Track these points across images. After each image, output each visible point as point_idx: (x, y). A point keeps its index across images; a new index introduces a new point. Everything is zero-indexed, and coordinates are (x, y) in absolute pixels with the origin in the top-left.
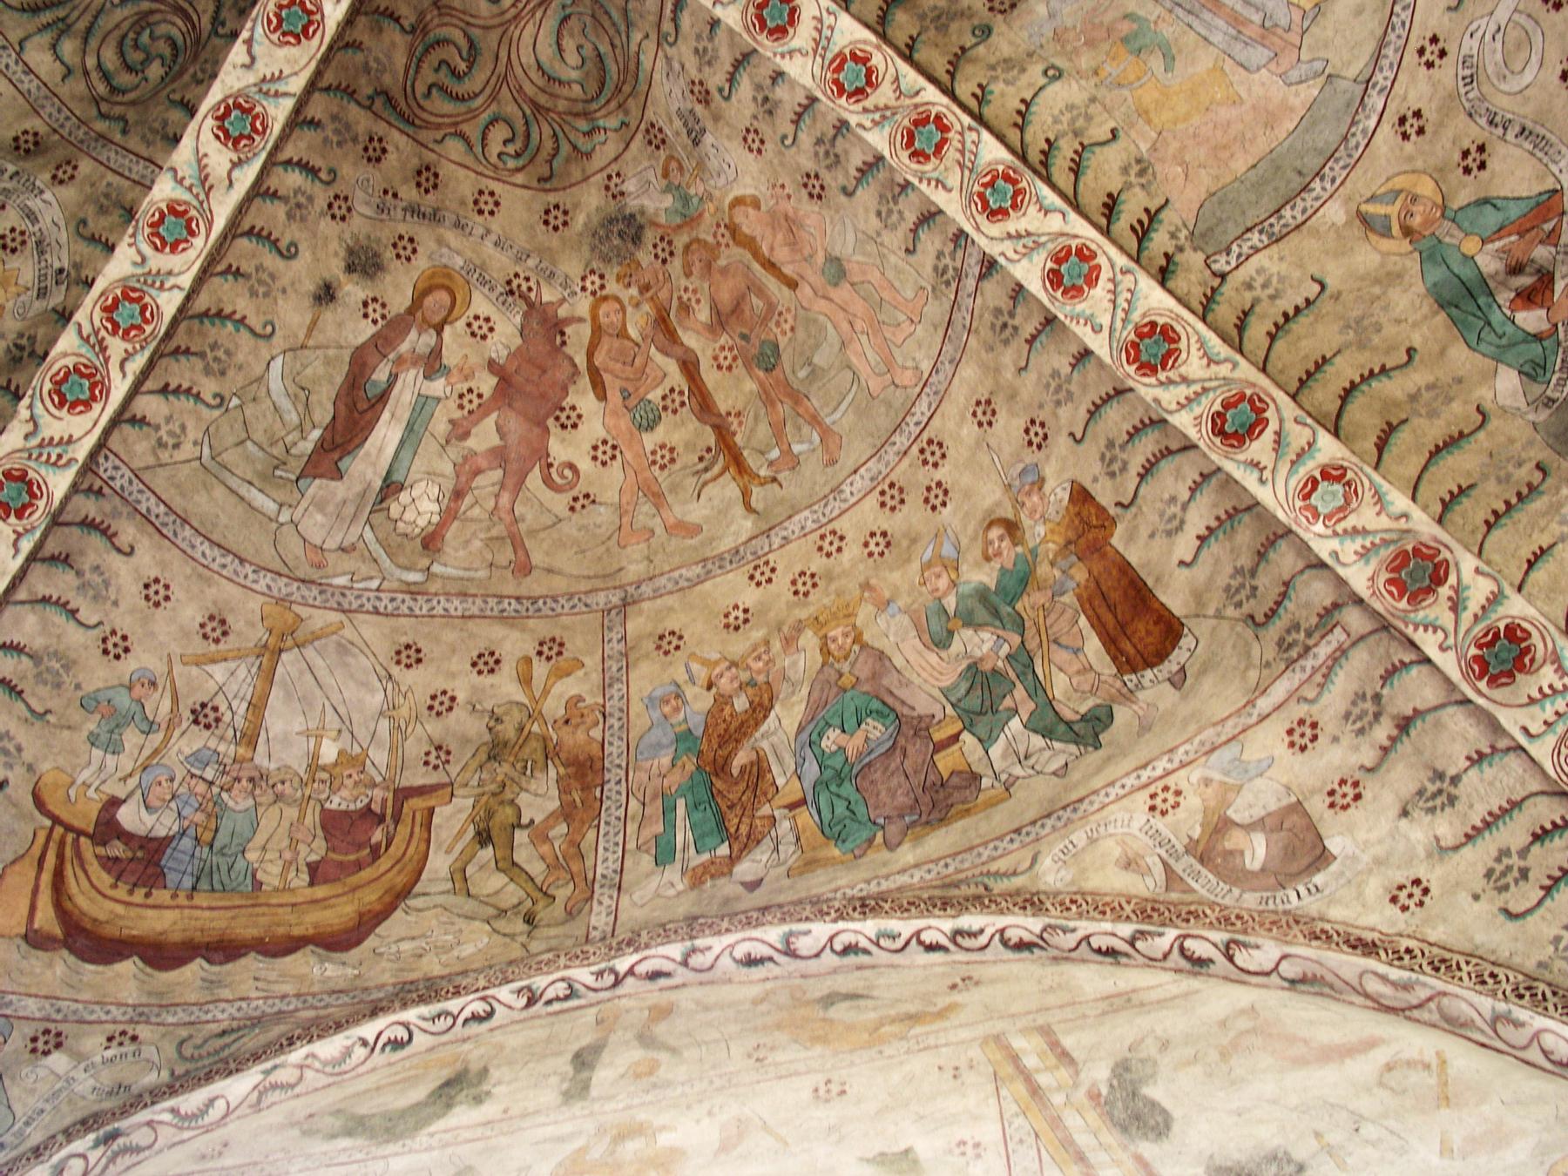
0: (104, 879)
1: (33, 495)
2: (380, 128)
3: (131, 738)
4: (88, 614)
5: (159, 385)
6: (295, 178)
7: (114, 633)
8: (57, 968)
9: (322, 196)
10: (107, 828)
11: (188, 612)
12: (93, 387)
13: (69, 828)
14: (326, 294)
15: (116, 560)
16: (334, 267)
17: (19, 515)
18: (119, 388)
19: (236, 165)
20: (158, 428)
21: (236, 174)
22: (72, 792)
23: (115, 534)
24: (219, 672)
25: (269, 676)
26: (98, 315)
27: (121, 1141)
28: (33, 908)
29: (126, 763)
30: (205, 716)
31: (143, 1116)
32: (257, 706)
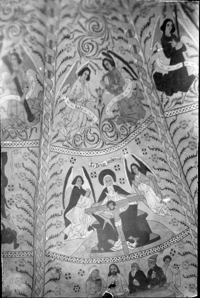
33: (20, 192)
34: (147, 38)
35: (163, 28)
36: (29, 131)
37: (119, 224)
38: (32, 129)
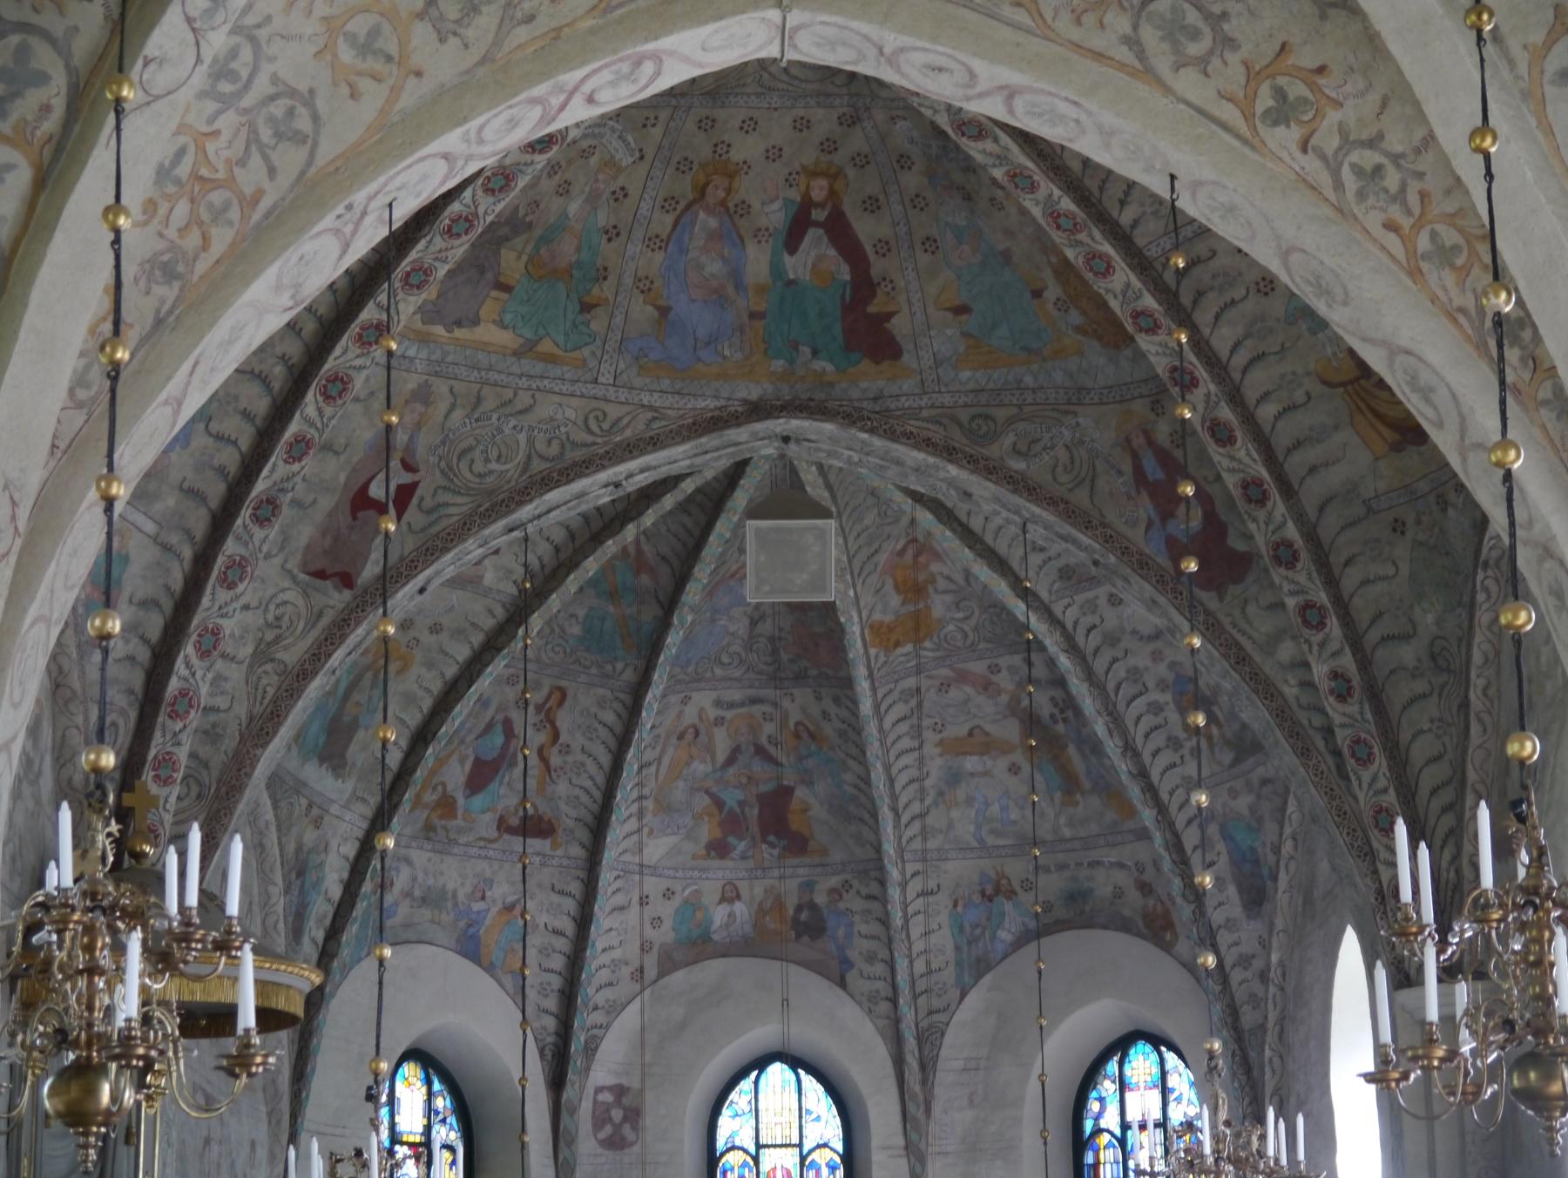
1: (1151, 316)
4: (1238, 293)
5: (1117, 205)
7: (1257, 283)
12: (1100, 257)
13: (1352, 382)
15: (1215, 264)
17: (1160, 328)
18: (1107, 248)
19: (996, 140)
20: (1144, 213)
21: (1002, 143)
22: (1334, 364)
23: (1199, 257)
26: (1059, 233)
27: (1491, 562)
28: (1380, 434)
31: (1485, 550)
33: (584, 758)
34: (870, 574)
35: (901, 553)
36: (619, 666)
37: (753, 813)
38: (627, 665)
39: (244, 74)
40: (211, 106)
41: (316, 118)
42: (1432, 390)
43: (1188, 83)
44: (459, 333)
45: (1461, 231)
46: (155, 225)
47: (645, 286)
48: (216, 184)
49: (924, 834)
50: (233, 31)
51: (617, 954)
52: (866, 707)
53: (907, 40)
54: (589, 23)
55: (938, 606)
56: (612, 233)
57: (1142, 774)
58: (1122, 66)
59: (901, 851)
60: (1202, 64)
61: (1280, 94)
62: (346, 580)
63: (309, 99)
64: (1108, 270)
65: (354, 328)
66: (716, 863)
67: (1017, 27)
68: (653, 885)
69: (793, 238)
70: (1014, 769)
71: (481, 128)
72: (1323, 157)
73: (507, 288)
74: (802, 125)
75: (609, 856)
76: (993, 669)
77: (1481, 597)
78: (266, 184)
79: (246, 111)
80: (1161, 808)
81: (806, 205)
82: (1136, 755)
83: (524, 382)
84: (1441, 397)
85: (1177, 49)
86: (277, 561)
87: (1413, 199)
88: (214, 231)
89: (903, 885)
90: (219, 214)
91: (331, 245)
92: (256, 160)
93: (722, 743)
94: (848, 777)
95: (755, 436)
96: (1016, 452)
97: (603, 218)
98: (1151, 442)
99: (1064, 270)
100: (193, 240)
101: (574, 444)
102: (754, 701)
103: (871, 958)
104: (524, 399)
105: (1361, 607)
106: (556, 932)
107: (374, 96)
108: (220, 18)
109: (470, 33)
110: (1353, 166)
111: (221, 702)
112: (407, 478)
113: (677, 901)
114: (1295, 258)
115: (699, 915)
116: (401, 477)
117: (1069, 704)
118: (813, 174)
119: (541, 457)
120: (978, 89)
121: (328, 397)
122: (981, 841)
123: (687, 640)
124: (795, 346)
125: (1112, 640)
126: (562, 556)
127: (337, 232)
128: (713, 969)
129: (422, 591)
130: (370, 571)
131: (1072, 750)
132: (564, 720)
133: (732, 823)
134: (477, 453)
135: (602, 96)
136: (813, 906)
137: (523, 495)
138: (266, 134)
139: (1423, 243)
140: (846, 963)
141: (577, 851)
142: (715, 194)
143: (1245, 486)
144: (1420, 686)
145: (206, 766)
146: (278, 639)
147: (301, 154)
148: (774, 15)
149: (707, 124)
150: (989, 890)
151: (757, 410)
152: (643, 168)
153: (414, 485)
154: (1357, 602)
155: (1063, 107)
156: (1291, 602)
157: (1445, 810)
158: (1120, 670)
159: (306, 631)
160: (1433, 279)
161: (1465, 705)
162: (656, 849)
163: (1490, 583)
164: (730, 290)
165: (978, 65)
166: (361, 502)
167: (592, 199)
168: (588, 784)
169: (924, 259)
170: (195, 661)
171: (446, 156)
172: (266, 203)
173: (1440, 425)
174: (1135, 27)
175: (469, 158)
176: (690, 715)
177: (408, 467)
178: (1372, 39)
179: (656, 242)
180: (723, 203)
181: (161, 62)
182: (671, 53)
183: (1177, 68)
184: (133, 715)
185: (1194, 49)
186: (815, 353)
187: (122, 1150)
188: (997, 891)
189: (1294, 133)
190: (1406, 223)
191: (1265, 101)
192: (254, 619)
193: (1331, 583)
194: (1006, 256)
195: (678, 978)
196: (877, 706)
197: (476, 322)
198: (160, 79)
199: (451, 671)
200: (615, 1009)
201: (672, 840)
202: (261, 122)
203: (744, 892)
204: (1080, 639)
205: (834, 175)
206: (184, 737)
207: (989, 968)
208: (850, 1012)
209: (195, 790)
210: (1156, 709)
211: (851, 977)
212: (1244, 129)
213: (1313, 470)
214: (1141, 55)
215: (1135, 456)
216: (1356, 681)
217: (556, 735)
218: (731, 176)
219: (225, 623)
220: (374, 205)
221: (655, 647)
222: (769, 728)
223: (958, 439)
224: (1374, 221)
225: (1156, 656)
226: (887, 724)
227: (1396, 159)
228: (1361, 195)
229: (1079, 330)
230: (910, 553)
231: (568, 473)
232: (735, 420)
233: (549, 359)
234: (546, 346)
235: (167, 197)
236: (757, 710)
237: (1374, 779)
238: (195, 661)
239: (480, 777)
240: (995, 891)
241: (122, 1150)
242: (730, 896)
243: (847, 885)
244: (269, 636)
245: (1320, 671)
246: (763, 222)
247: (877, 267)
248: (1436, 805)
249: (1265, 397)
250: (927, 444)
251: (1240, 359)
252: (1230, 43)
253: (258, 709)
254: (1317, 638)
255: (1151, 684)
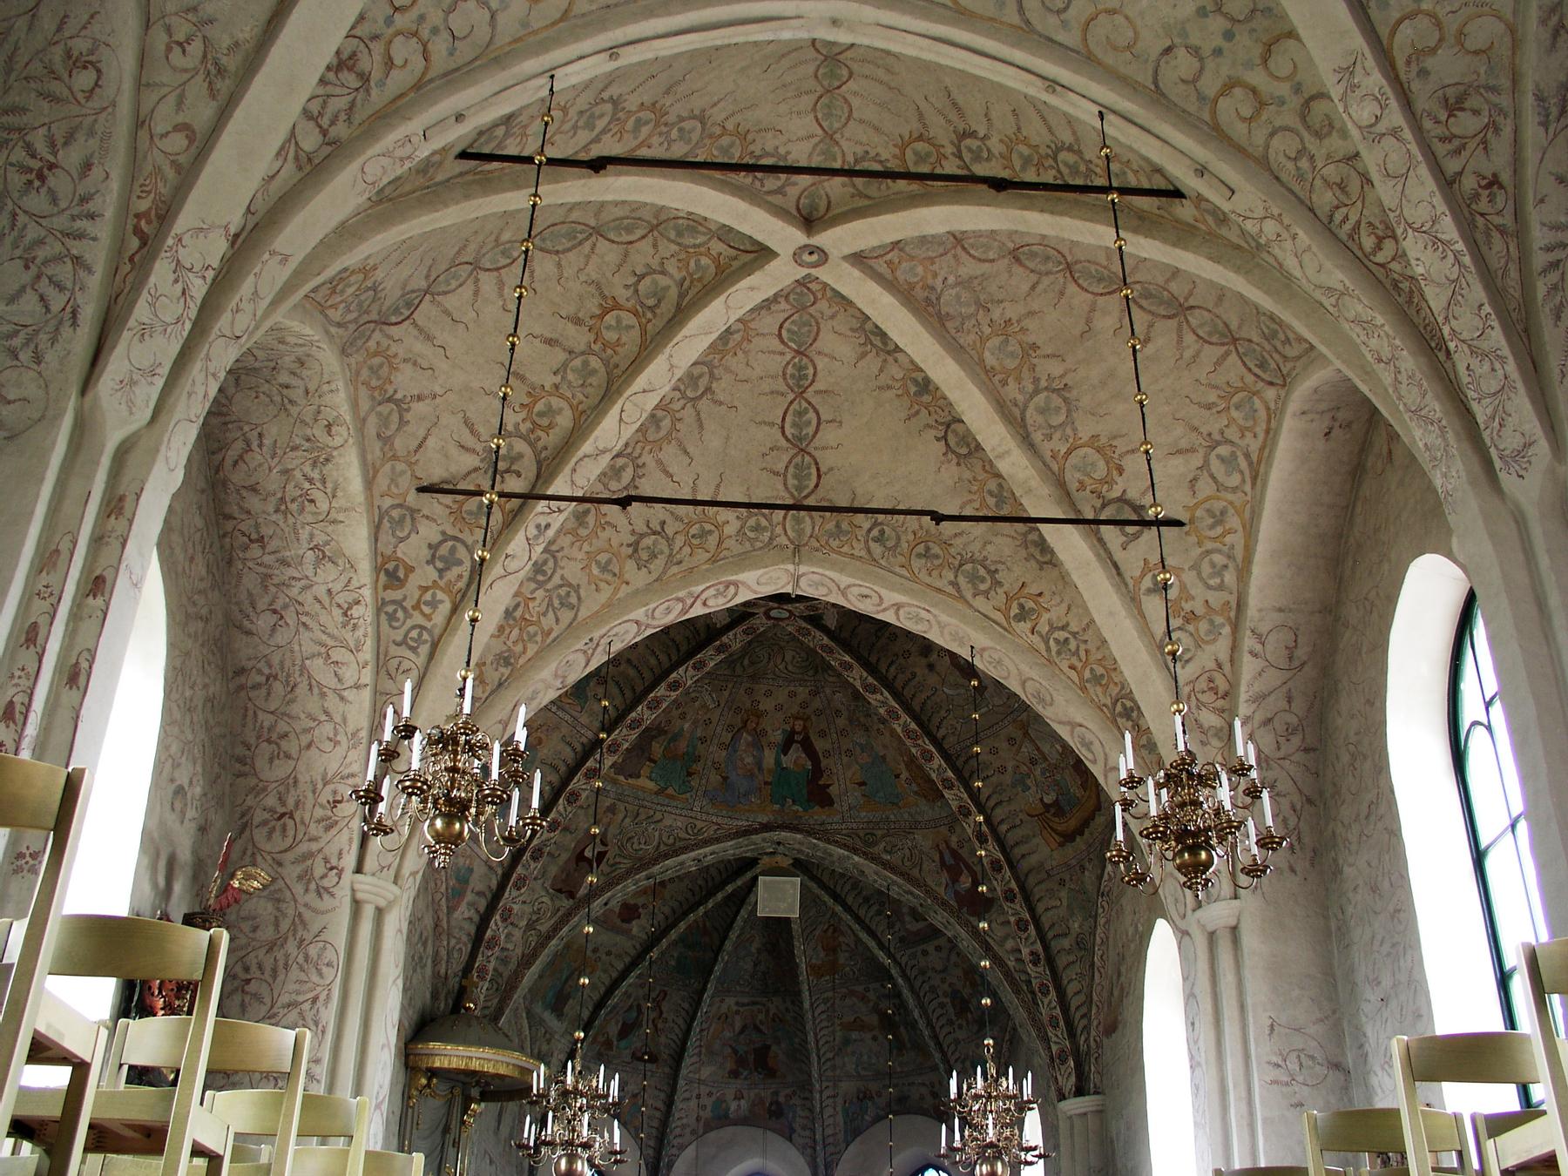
0: (1057, 820)
2: (887, 634)
3: (1028, 782)
6: (892, 669)
8: (1069, 850)
9: (901, 660)
10: (1047, 807)
11: (1005, 745)
14: (931, 667)
16: (924, 661)
24: (1023, 749)
25: (1032, 741)
29: (1034, 788)
30: (1033, 762)
32: (1038, 749)
35: (825, 931)
37: (751, 1058)
39: (549, 573)
40: (533, 586)
41: (579, 598)
42: (1091, 743)
43: (979, 603)
44: (630, 781)
45: (1104, 667)
46: (503, 638)
47: (716, 766)
48: (532, 623)
49: (834, 1068)
50: (546, 550)
51: (685, 1121)
52: (807, 1005)
53: (851, 581)
54: (704, 567)
55: (842, 958)
56: (703, 740)
57: (935, 1037)
58: (950, 595)
59: (820, 1076)
60: (986, 594)
61: (1021, 607)
62: (571, 895)
63: (577, 589)
64: (931, 759)
65: (584, 770)
66: (732, 1081)
67: (902, 576)
68: (704, 1090)
69: (785, 749)
70: (875, 1039)
71: (654, 610)
72: (1042, 636)
73: (654, 762)
74: (792, 695)
75: (684, 1072)
76: (867, 990)
77: (1100, 910)
78: (554, 626)
79: (547, 591)
80: (944, 1054)
81: (793, 732)
82: (933, 1028)
83: (659, 807)
84: (1096, 747)
85: (975, 586)
86: (540, 882)
87: (1082, 654)
88: (529, 645)
89: (821, 1092)
90: (532, 637)
91: (582, 659)
92: (551, 614)
93: (738, 1025)
94: (797, 1040)
95: (764, 840)
96: (886, 851)
97: (699, 733)
98: (948, 847)
99: (911, 762)
100: (519, 648)
101: (681, 839)
102: (754, 1003)
103: (804, 1128)
104: (658, 816)
105: (1046, 920)
106: (656, 1108)
107: (606, 592)
108: (541, 540)
109: (652, 567)
110: (1055, 639)
111: (510, 946)
112: (602, 849)
113: (714, 1098)
114: (1029, 684)
115: (724, 1105)
116: (599, 848)
117: (902, 1006)
118: (797, 718)
119: (666, 845)
120: (884, 606)
121: (569, 802)
122: (858, 1073)
123: (724, 970)
124: (785, 798)
125: (923, 972)
126: (670, 921)
127: (585, 652)
128: (730, 1129)
129: (606, 904)
130: (582, 892)
131: (902, 1029)
132: (665, 1007)
133: (741, 1062)
134: (635, 840)
135: (710, 602)
136: (777, 1103)
137: (655, 861)
138: (556, 603)
139: (1087, 674)
140: (793, 1131)
141: (667, 1070)
142: (750, 725)
143: (992, 863)
144: (1072, 958)
145: (501, 975)
146: (537, 920)
147: (571, 614)
148: (791, 567)
149: (749, 692)
150: (861, 1096)
151: (766, 827)
152: (719, 710)
153: (606, 852)
154: (1043, 919)
155: (923, 614)
156: (1012, 919)
157: (1082, 1017)
158: (926, 987)
159: (551, 918)
160: (1091, 691)
161: (1093, 964)
162: (706, 1072)
163: (1104, 903)
164: (756, 771)
165: (883, 592)
166: (580, 857)
167: (695, 723)
168: (675, 1038)
169: (845, 759)
170: (499, 923)
171: (637, 622)
172: (554, 635)
173: (1094, 762)
174: (956, 577)
175: (648, 626)
176: (724, 1009)
177: (604, 843)
178: (1064, 578)
179: (722, 746)
180: (755, 729)
181: (513, 557)
182: (743, 583)
183: (975, 596)
184: (470, 946)
185: (983, 587)
186: (794, 801)
187: (451, 1148)
188: (865, 1097)
189: (1029, 625)
190: (1079, 665)
191: (1015, 610)
192: (528, 909)
193: (1032, 910)
194: (884, 757)
195: (712, 1135)
196: (812, 1005)
197: (639, 777)
198: (513, 565)
199: (615, 975)
200: (682, 1148)
201: (713, 1068)
202: (554, 596)
203: (745, 1095)
204: (908, 972)
205: (806, 719)
206: (492, 959)
207: (860, 1134)
208: (793, 1153)
209: (495, 986)
210: (942, 1005)
211: (795, 1136)
212: (1005, 624)
213: (1023, 856)
214: (959, 590)
215: (941, 853)
216: (1042, 956)
217: (661, 1013)
218: (758, 717)
219: (514, 906)
220: (602, 641)
221: (710, 972)
222: (761, 1017)
223: (859, 844)
224: (1064, 665)
225: (943, 981)
226: (816, 1014)
227: (1074, 634)
228: (1059, 653)
229: (916, 793)
230: (831, 930)
231: (677, 853)
232: (756, 832)
233: (671, 797)
234: (670, 791)
235: (509, 625)
236: (755, 1008)
237: (1050, 1002)
238: (499, 923)
239: (625, 1031)
240: (864, 1097)
241: (451, 1148)
242: (739, 1096)
243: (794, 1093)
244: (534, 918)
245: (1025, 951)
246: (772, 739)
247: (824, 763)
248: (1078, 1016)
249: (1002, 821)
250: (845, 846)
251: (992, 803)
252: (1000, 584)
253: (527, 952)
254: (1024, 936)
255: (940, 993)
